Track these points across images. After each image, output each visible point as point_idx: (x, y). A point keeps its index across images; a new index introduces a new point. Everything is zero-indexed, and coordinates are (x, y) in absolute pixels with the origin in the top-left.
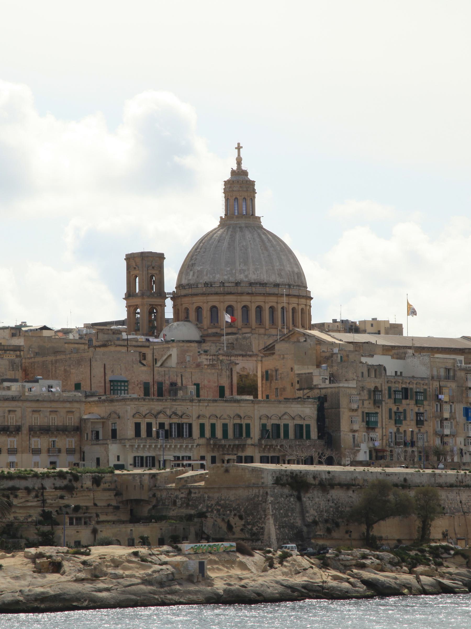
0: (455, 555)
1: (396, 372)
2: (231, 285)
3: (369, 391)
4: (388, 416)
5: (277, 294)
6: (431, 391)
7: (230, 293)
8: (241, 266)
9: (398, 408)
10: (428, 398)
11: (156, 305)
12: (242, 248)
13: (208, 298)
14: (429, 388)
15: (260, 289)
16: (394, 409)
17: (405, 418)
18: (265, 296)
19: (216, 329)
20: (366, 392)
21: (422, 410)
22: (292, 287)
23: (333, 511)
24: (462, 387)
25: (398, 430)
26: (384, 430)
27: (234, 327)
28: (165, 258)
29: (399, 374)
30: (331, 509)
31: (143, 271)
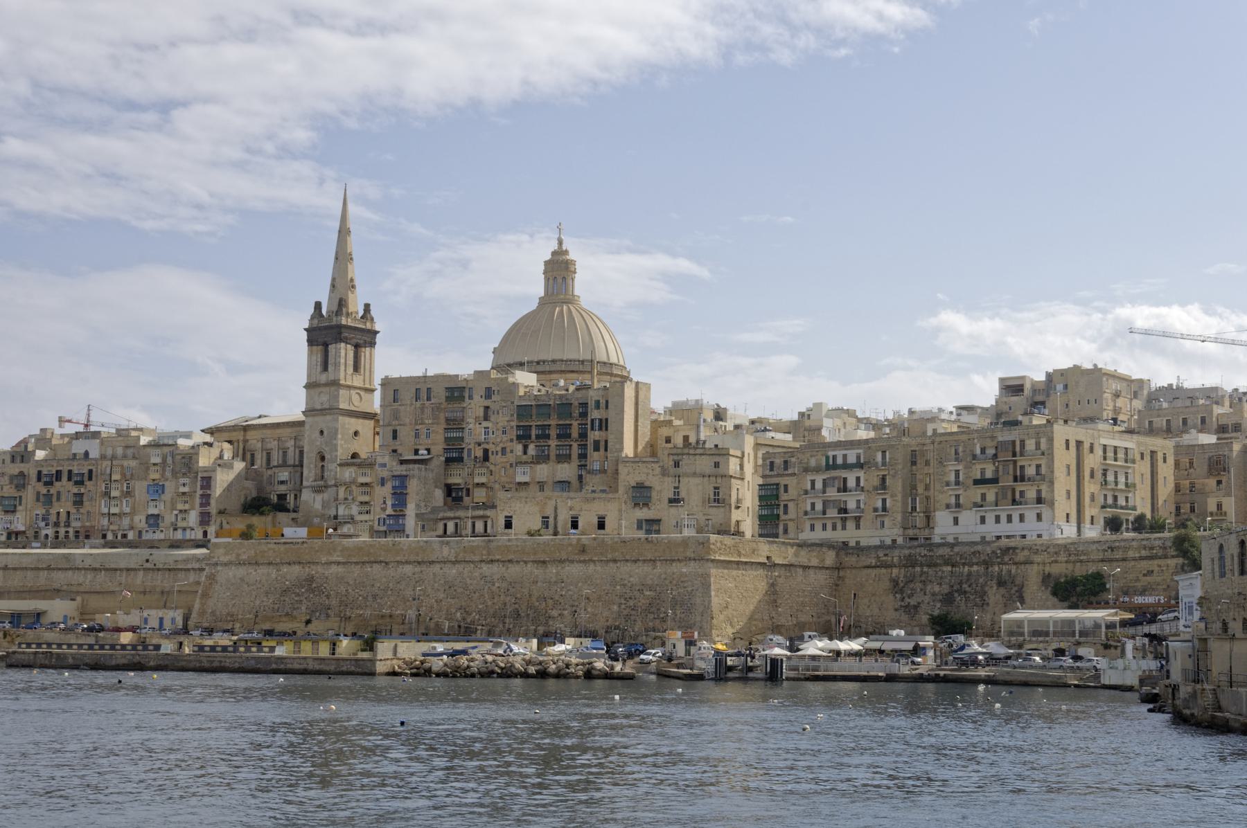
6: (99, 471)
9: (48, 491)
10: (94, 478)
16: (44, 491)
17: (58, 499)
20: (6, 478)
21: (83, 490)
25: (47, 511)
26: (28, 513)
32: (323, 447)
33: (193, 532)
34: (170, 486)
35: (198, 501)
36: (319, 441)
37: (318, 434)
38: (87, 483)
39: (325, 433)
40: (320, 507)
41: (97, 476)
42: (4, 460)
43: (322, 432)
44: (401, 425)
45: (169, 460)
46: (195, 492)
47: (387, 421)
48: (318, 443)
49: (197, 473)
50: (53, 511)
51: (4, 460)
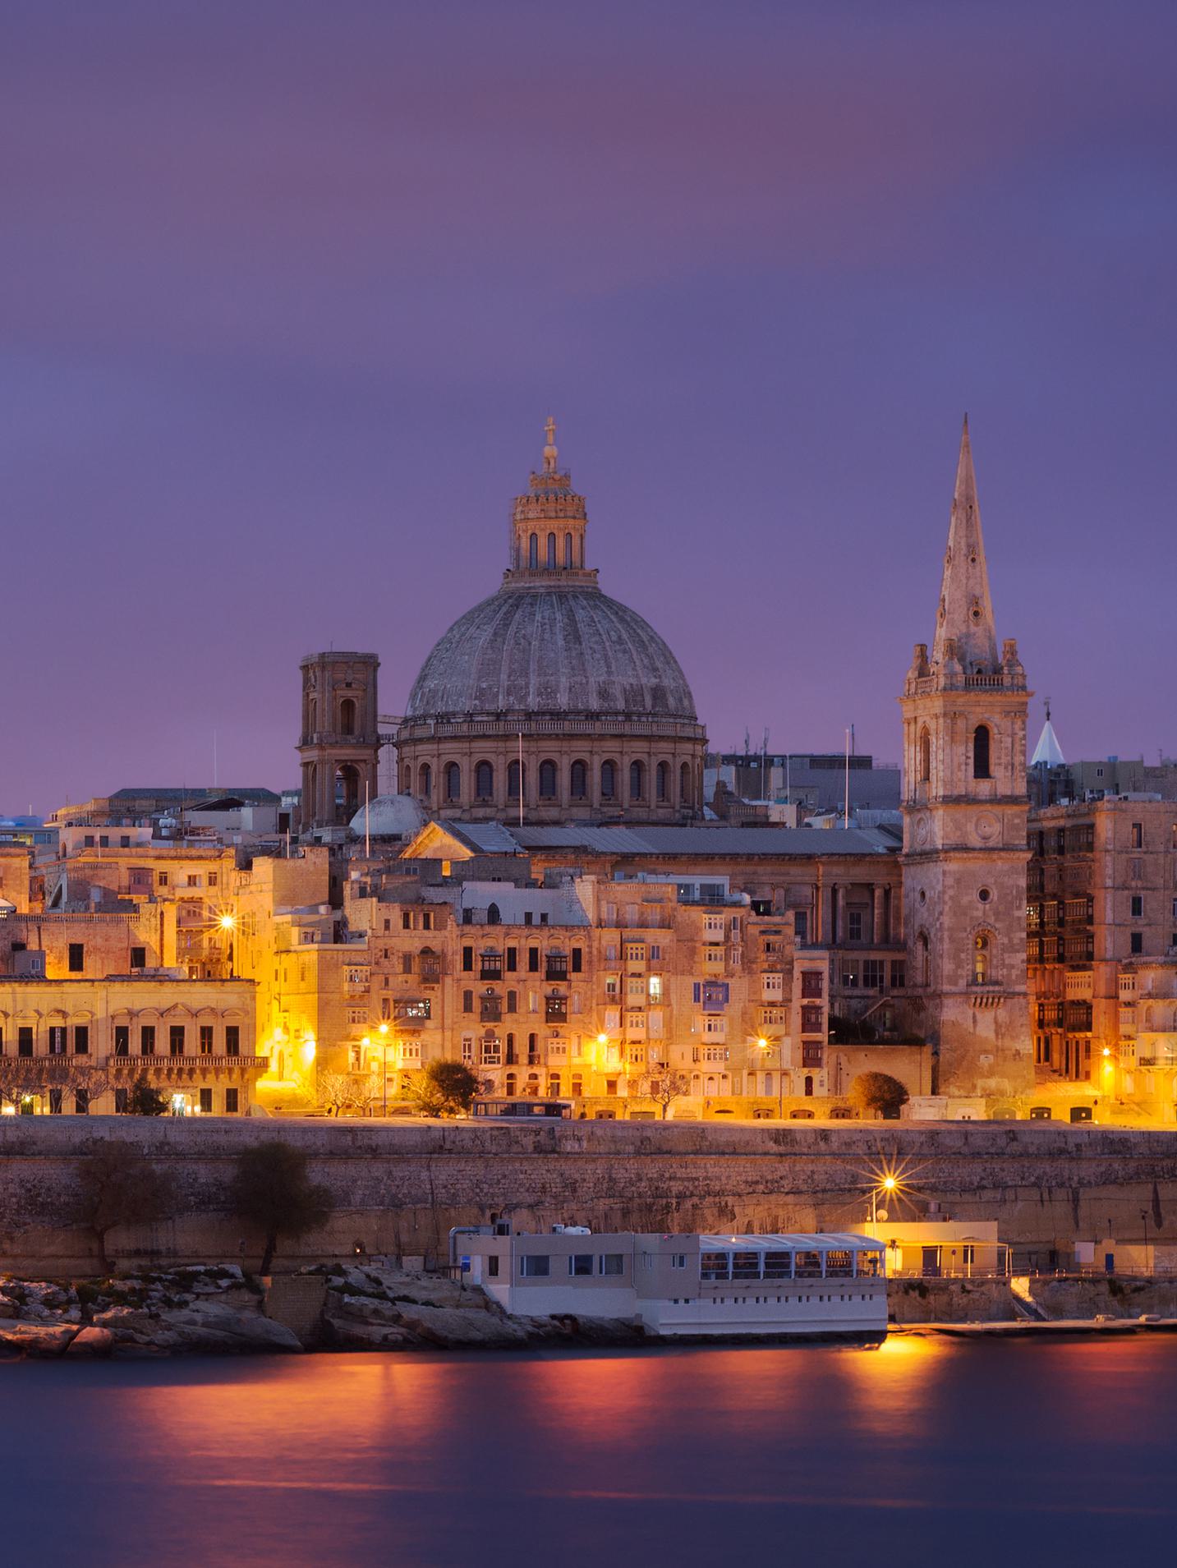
0: (229, 1288)
1: (528, 916)
2: (485, 719)
3: (407, 959)
4: (461, 1007)
5: (589, 735)
6: (595, 952)
7: (485, 737)
8: (512, 678)
11: (352, 761)
12: (522, 641)
13: (442, 746)
14: (590, 947)
15: (548, 727)
17: (512, 1008)
18: (562, 740)
19: (454, 810)
22: (635, 718)
23: (18, 1203)
24: (692, 940)
25: (490, 1035)
27: (491, 806)
28: (379, 664)
29: (536, 920)
30: (14, 1200)
31: (323, 692)
32: (992, 920)
33: (785, 1079)
34: (739, 987)
35: (796, 1020)
36: (980, 909)
37: (976, 896)
38: (573, 976)
39: (994, 895)
40: (992, 1035)
41: (590, 962)
42: (387, 922)
43: (984, 895)
44: (1148, 889)
45: (736, 935)
46: (790, 1001)
47: (1119, 881)
48: (979, 914)
49: (791, 963)
50: (501, 1031)
51: (387, 922)
